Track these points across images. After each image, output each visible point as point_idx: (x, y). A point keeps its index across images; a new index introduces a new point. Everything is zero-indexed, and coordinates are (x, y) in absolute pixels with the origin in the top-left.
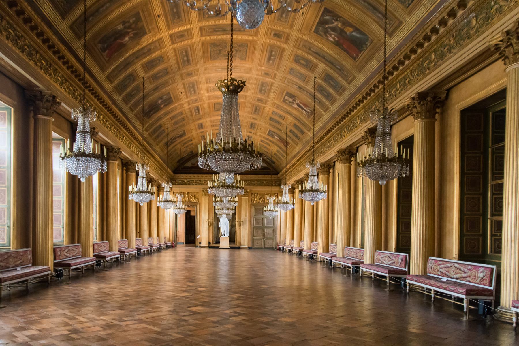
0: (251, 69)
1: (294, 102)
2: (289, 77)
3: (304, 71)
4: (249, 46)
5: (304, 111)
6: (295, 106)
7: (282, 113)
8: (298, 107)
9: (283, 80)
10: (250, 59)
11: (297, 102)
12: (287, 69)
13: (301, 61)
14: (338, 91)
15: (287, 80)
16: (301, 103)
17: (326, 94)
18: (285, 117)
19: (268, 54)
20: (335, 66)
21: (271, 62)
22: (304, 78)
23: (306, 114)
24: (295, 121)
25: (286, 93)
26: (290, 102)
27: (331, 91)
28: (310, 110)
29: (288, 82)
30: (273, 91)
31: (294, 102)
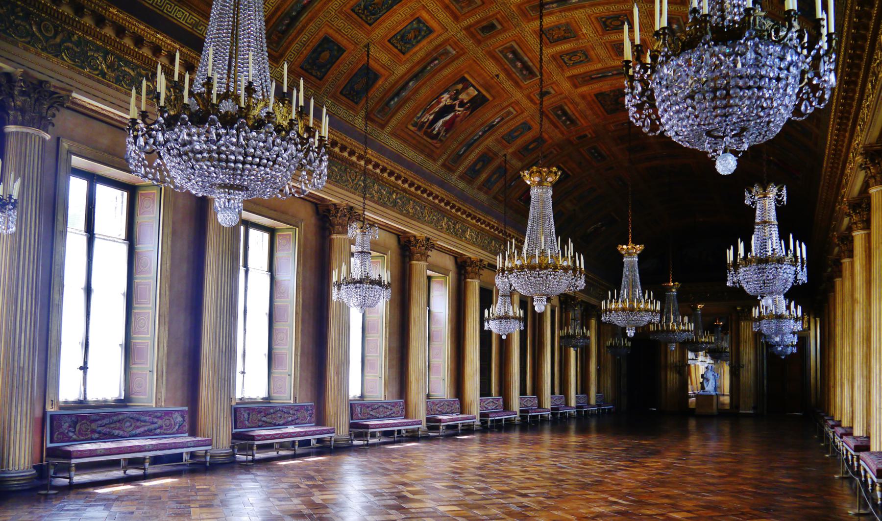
0: (576, 87)
1: (457, 102)
2: (519, 120)
3: (520, 142)
4: (606, 114)
5: (432, 117)
6: (446, 99)
7: (422, 54)
8: (441, 105)
9: (517, 108)
10: (589, 99)
11: (457, 108)
12: (532, 123)
13: (535, 144)
14: (483, 185)
15: (515, 113)
16: (456, 116)
17: (477, 168)
18: (404, 53)
19: (574, 117)
20: (515, 180)
21: (559, 112)
22: (509, 138)
23: (424, 119)
24: (392, 79)
25: (484, 96)
26: (458, 93)
27: (484, 176)
28: (439, 133)
29: (509, 113)
30: (502, 76)
31: (457, 102)
